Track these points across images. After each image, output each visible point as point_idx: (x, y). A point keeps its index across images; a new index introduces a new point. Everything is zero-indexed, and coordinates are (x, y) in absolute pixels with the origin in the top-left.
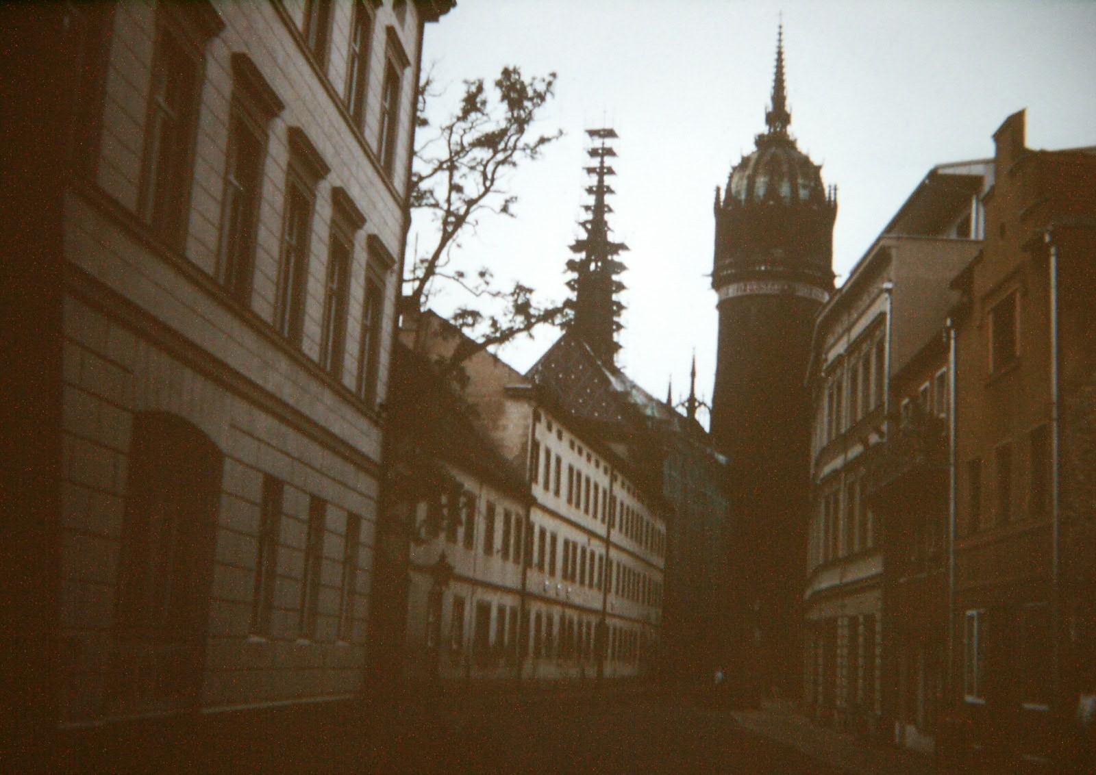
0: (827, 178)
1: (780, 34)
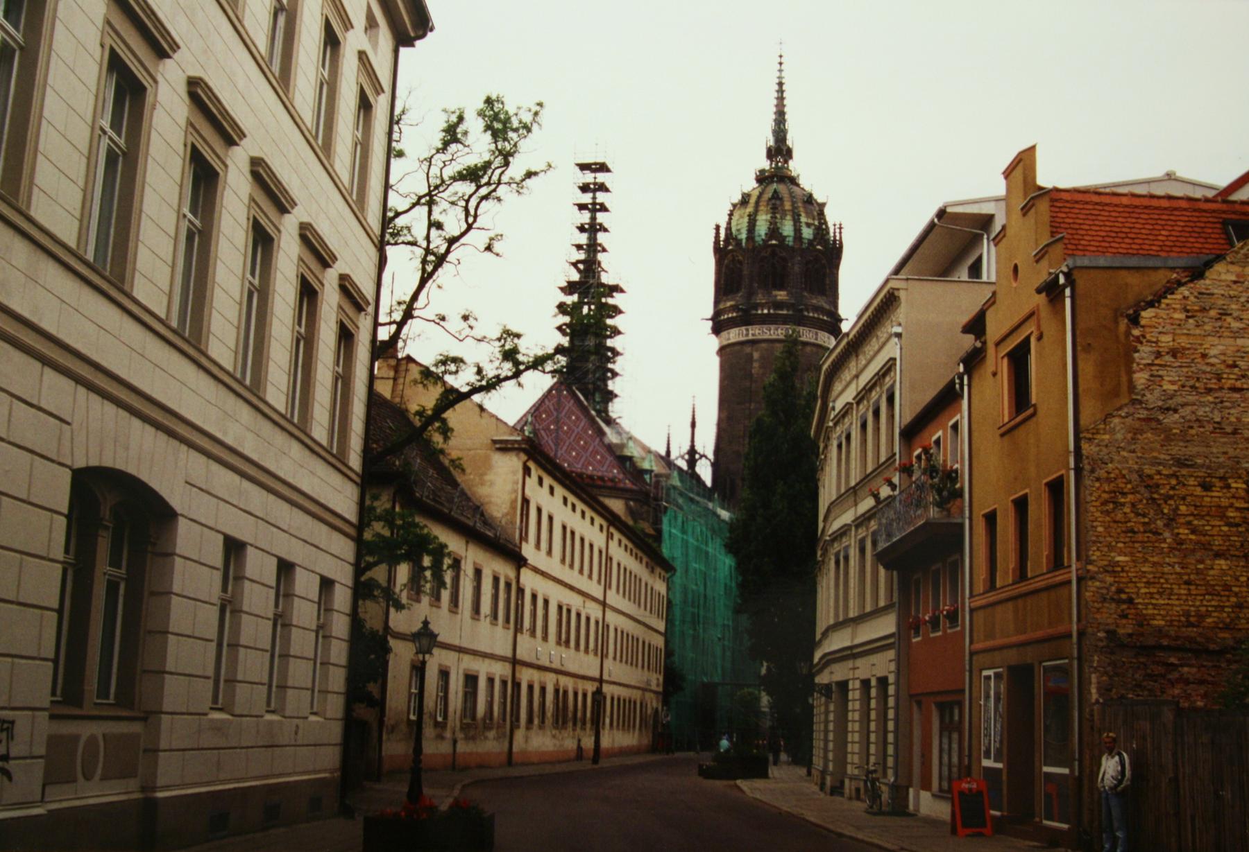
0: (832, 217)
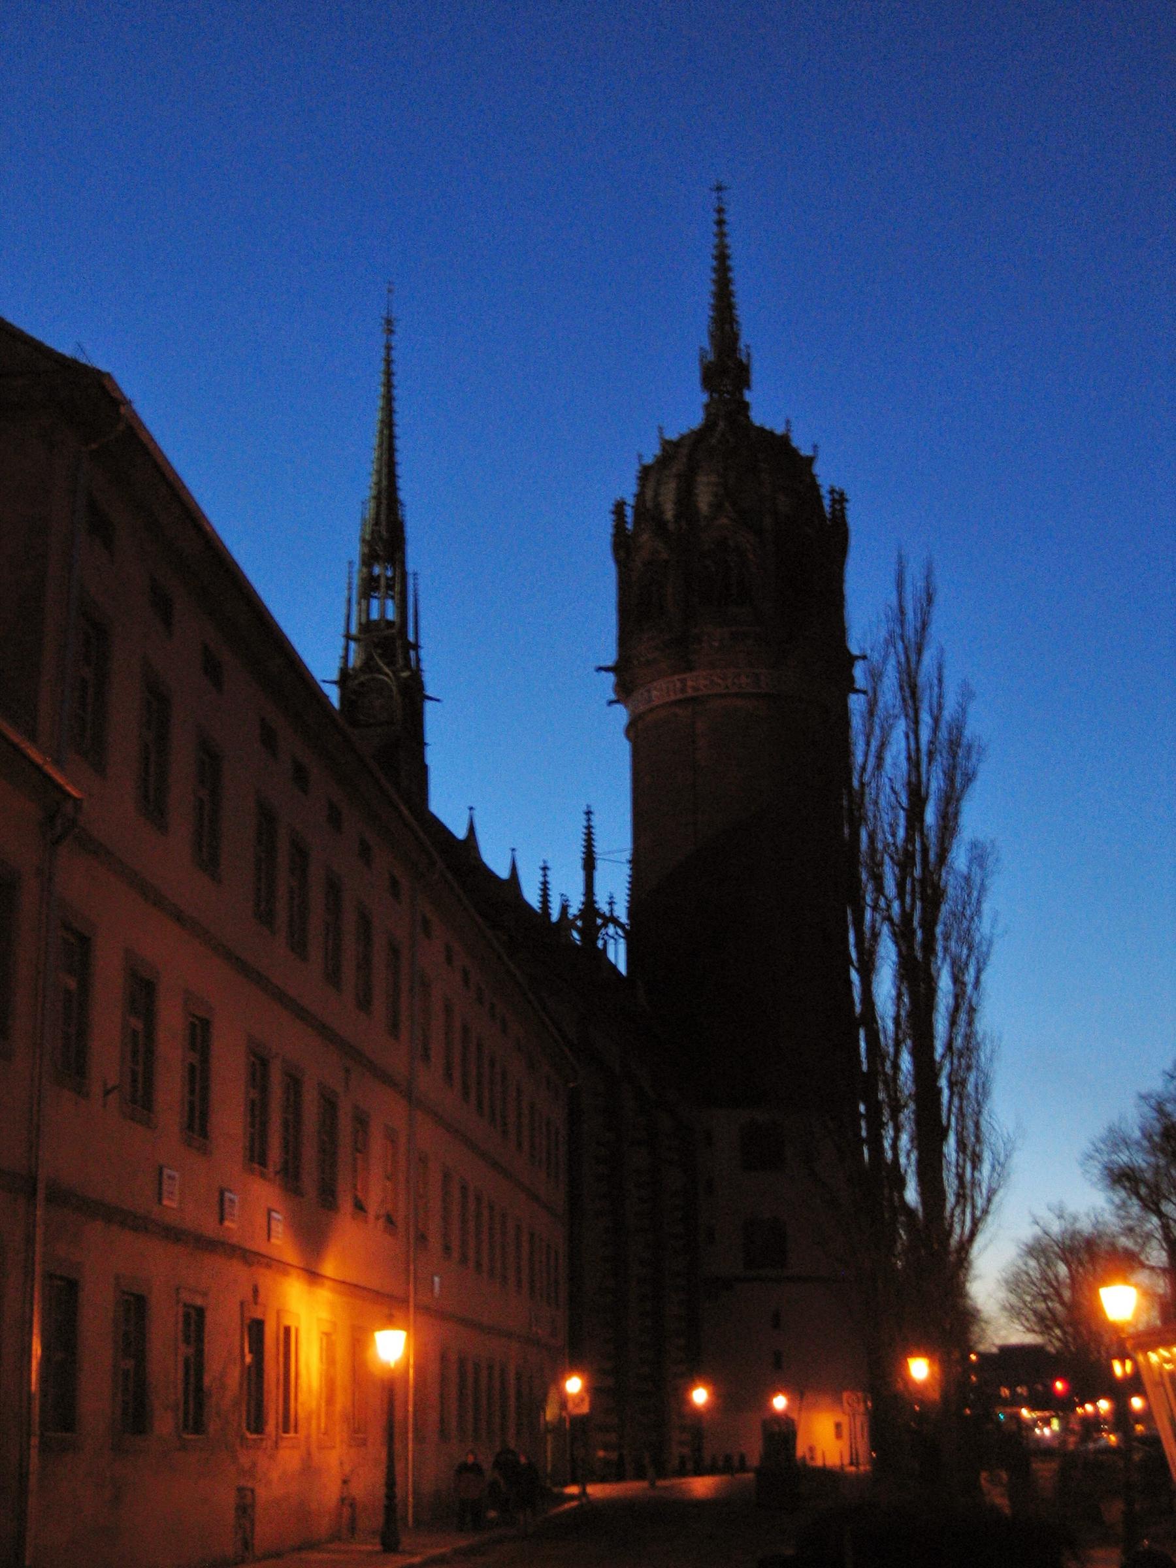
1: (720, 223)
